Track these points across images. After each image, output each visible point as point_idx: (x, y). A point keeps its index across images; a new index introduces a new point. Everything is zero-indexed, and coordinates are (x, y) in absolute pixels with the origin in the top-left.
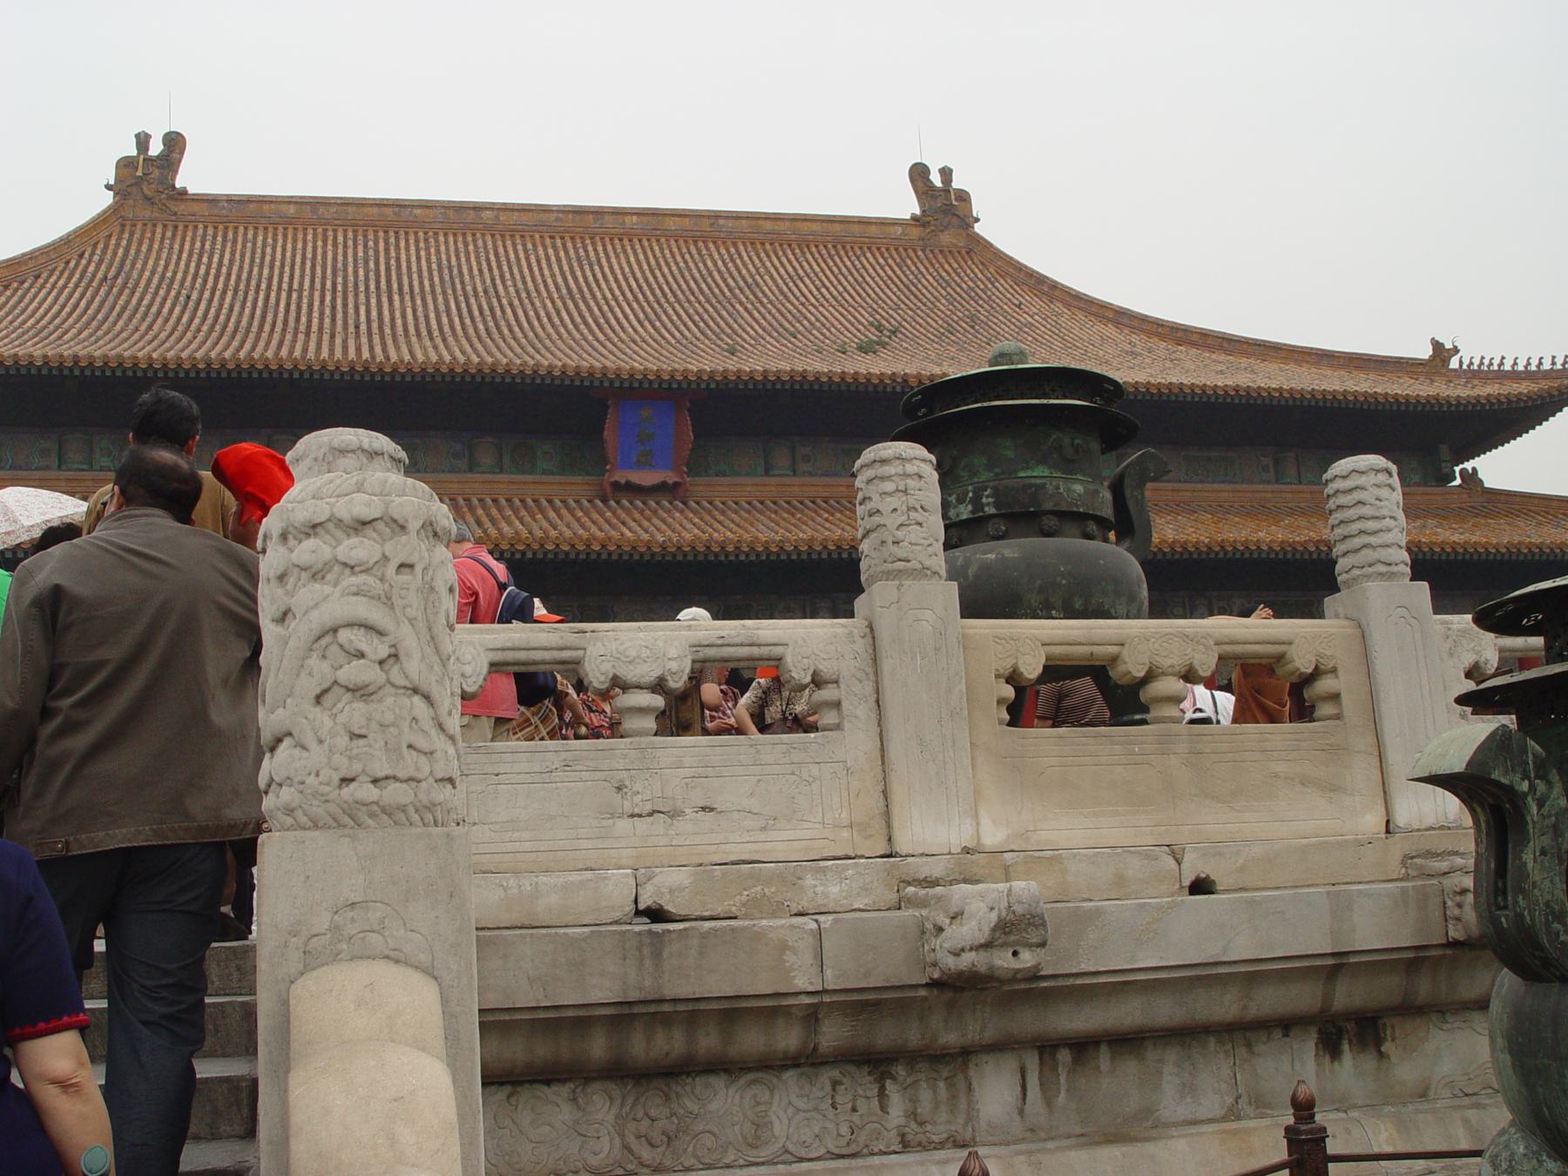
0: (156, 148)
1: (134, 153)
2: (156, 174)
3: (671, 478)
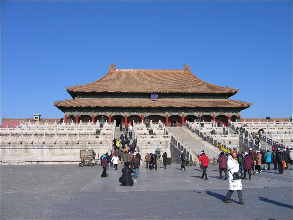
3: (156, 99)
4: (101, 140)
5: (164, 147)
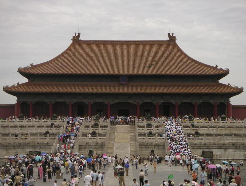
0: (77, 35)
1: (74, 35)
2: (77, 38)
4: (48, 141)
5: (100, 147)
